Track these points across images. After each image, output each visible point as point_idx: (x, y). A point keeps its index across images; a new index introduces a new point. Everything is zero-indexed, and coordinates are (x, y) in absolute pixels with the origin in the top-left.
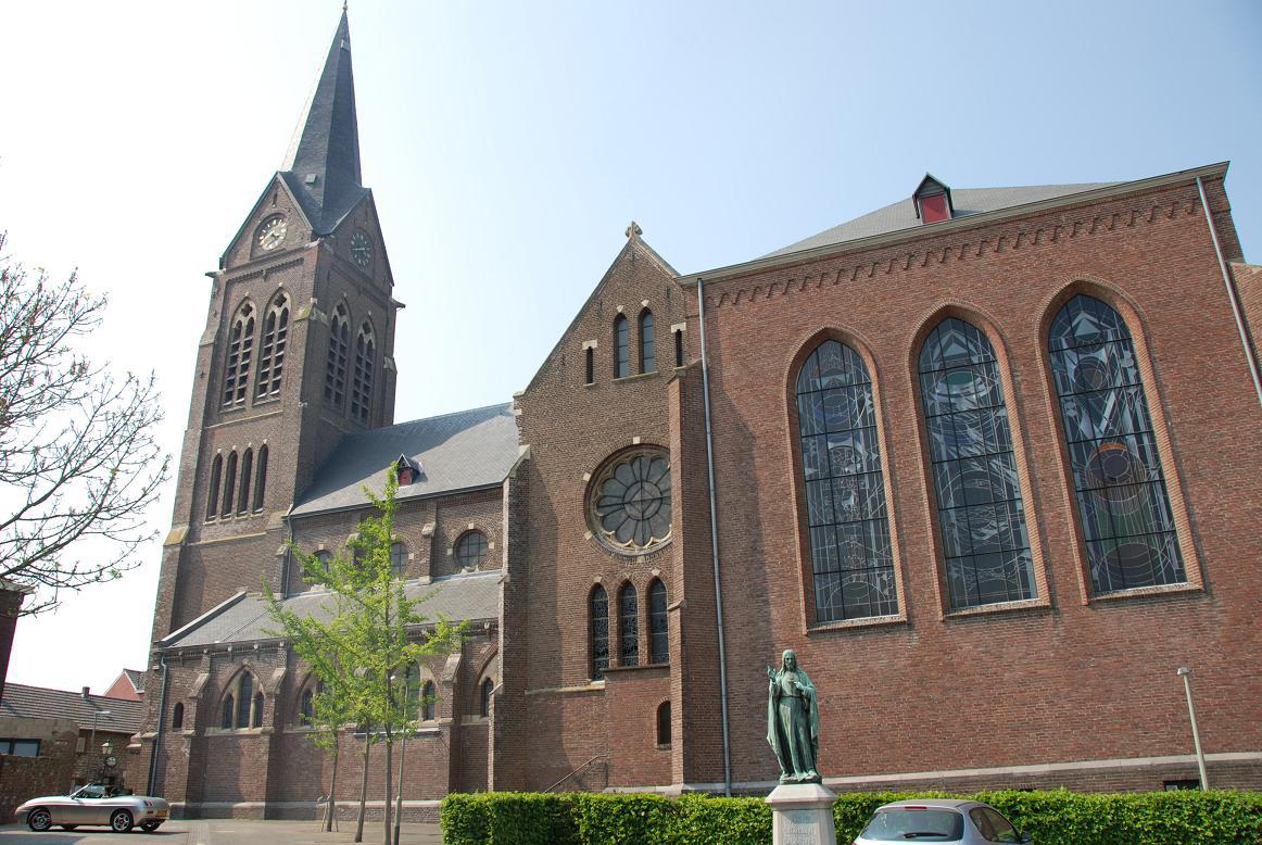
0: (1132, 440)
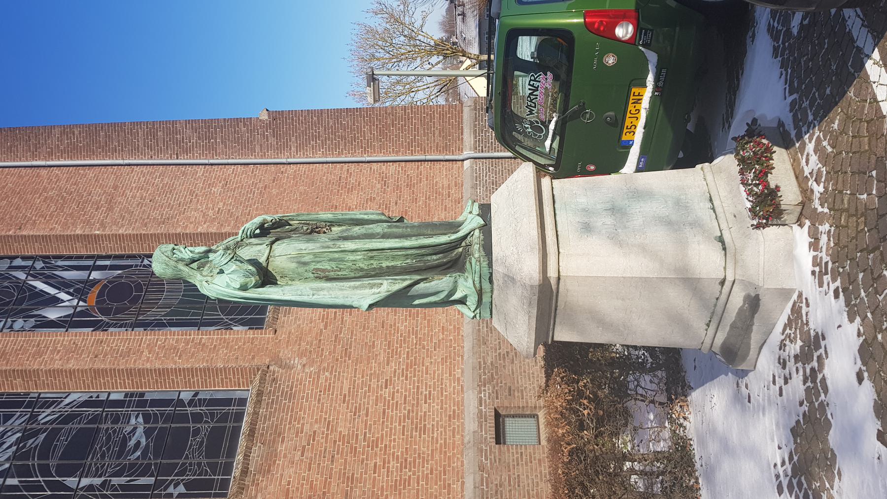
0: (95, 275)
